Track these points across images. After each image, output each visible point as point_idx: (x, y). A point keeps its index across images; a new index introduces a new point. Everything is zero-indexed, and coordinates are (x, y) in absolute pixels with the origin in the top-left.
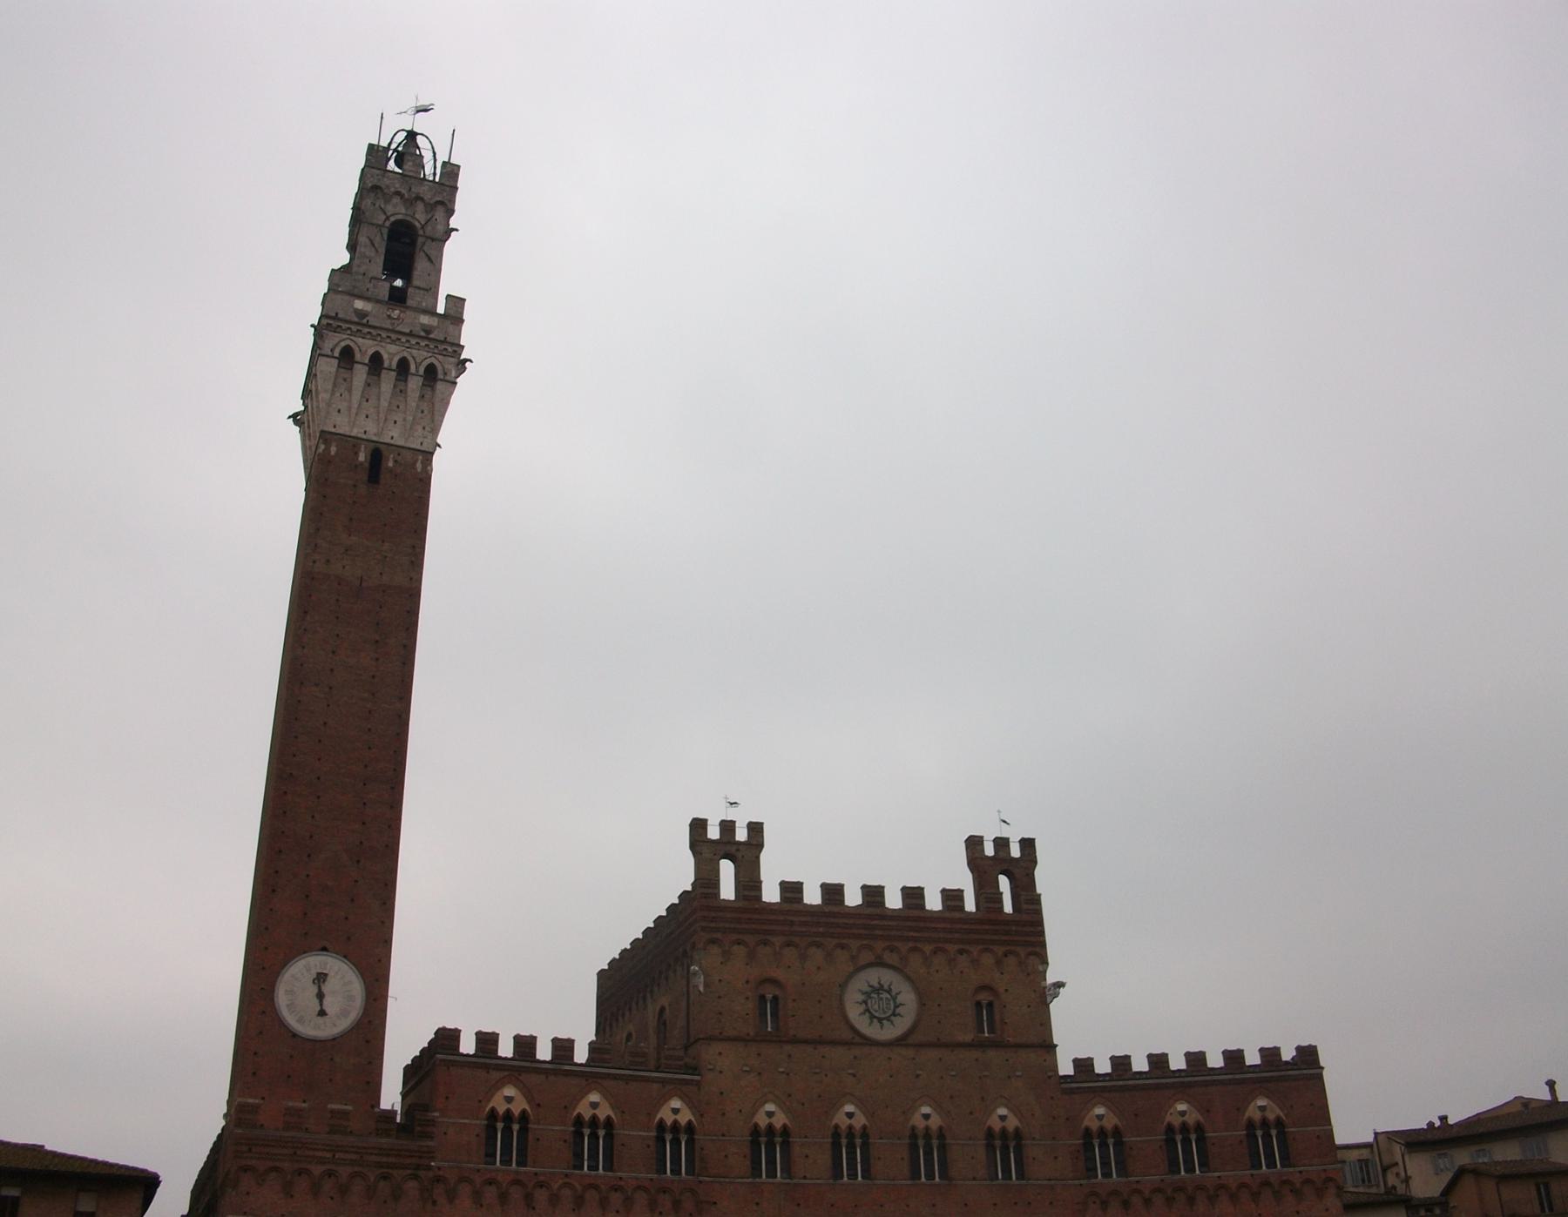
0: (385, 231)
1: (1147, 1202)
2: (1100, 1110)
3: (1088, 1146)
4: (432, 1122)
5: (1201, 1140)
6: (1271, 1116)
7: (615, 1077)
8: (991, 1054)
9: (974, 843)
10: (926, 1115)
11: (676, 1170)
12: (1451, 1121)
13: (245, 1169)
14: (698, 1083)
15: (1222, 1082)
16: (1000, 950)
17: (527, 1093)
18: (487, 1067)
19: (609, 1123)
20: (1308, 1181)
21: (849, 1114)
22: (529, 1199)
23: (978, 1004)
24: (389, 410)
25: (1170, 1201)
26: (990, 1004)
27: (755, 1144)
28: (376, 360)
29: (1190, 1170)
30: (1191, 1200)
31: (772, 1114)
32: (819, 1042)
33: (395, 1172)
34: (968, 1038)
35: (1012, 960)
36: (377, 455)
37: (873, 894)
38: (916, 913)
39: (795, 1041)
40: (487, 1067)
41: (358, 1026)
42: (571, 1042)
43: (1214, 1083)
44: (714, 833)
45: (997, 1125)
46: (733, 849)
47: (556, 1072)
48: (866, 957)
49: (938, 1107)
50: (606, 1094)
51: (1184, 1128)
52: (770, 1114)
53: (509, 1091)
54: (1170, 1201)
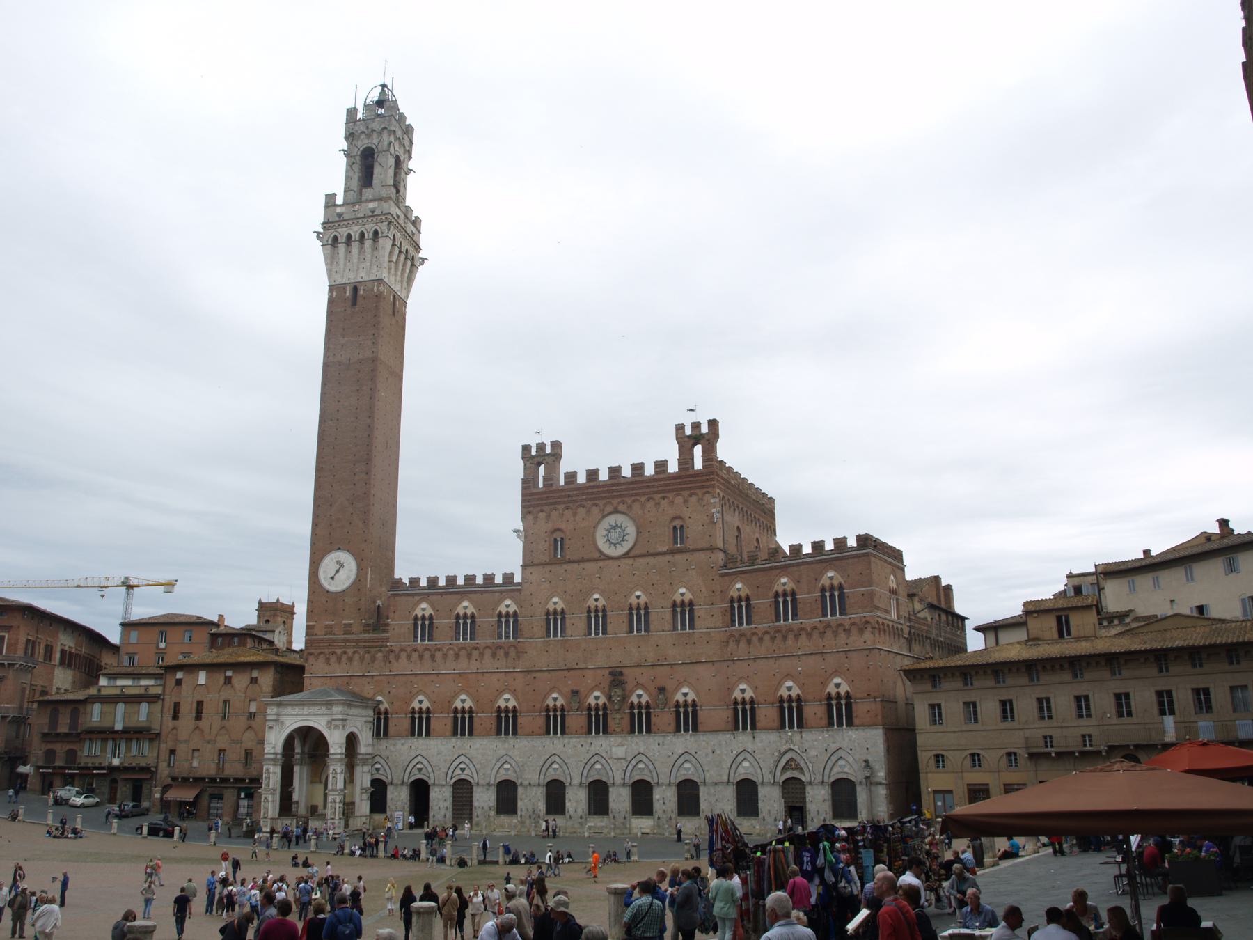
0: (358, 158)
1: (761, 640)
2: (739, 585)
3: (732, 608)
4: (387, 625)
5: (794, 601)
6: (836, 583)
7: (476, 592)
8: (678, 557)
9: (680, 428)
10: (639, 596)
11: (507, 637)
12: (1153, 553)
13: (311, 654)
14: (519, 591)
15: (808, 563)
16: (686, 493)
17: (433, 606)
18: (413, 595)
19: (473, 616)
20: (854, 624)
21: (596, 599)
22: (433, 657)
23: (675, 528)
24: (359, 262)
25: (773, 639)
26: (682, 527)
27: (548, 620)
28: (349, 237)
29: (786, 619)
30: (785, 638)
31: (556, 603)
32: (582, 560)
33: (372, 650)
34: (665, 549)
35: (694, 498)
36: (355, 289)
37: (615, 471)
38: (637, 479)
39: (570, 562)
40: (413, 595)
41: (354, 583)
42: (456, 577)
43: (802, 564)
44: (534, 452)
45: (678, 599)
46: (540, 459)
47: (446, 593)
48: (609, 509)
49: (645, 591)
50: (470, 601)
51: (785, 594)
52: (555, 603)
53: (424, 605)
54: (773, 639)
